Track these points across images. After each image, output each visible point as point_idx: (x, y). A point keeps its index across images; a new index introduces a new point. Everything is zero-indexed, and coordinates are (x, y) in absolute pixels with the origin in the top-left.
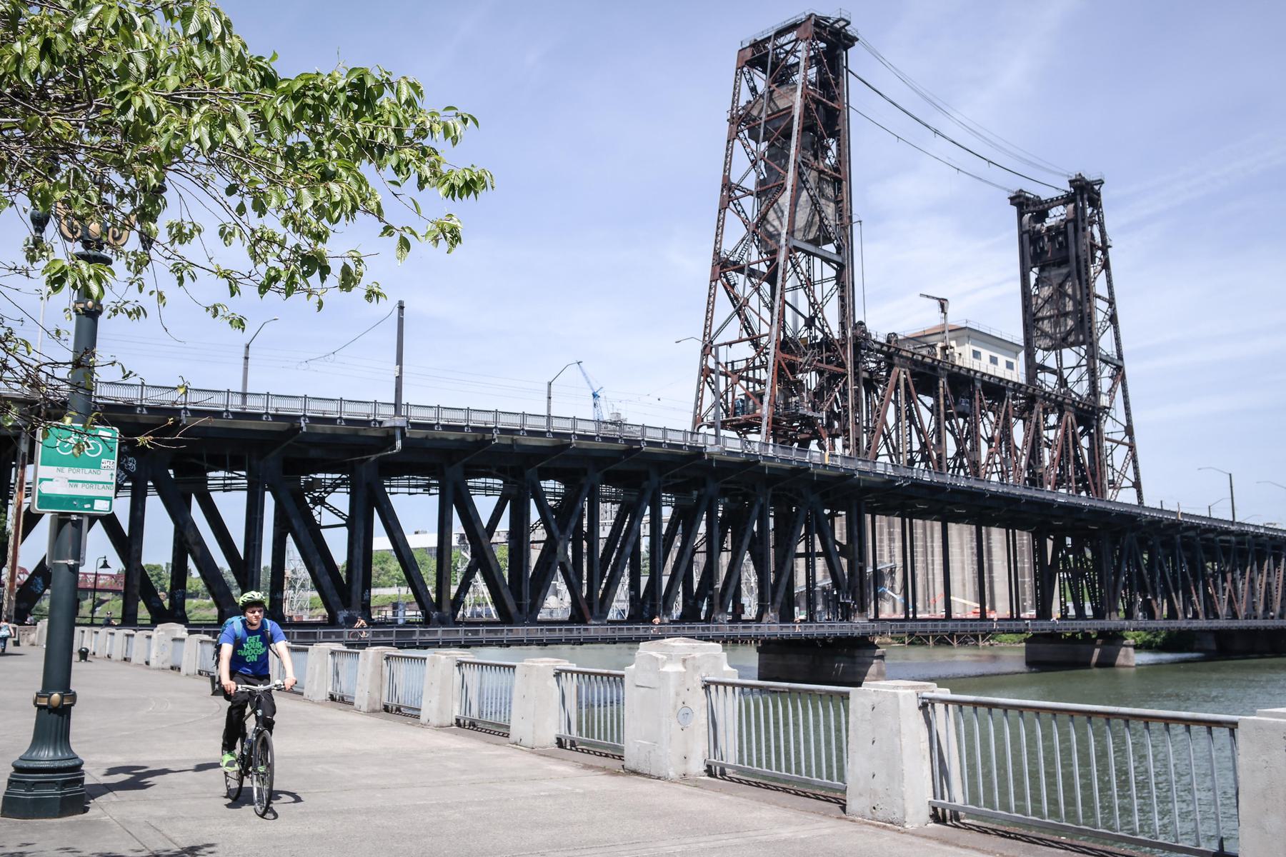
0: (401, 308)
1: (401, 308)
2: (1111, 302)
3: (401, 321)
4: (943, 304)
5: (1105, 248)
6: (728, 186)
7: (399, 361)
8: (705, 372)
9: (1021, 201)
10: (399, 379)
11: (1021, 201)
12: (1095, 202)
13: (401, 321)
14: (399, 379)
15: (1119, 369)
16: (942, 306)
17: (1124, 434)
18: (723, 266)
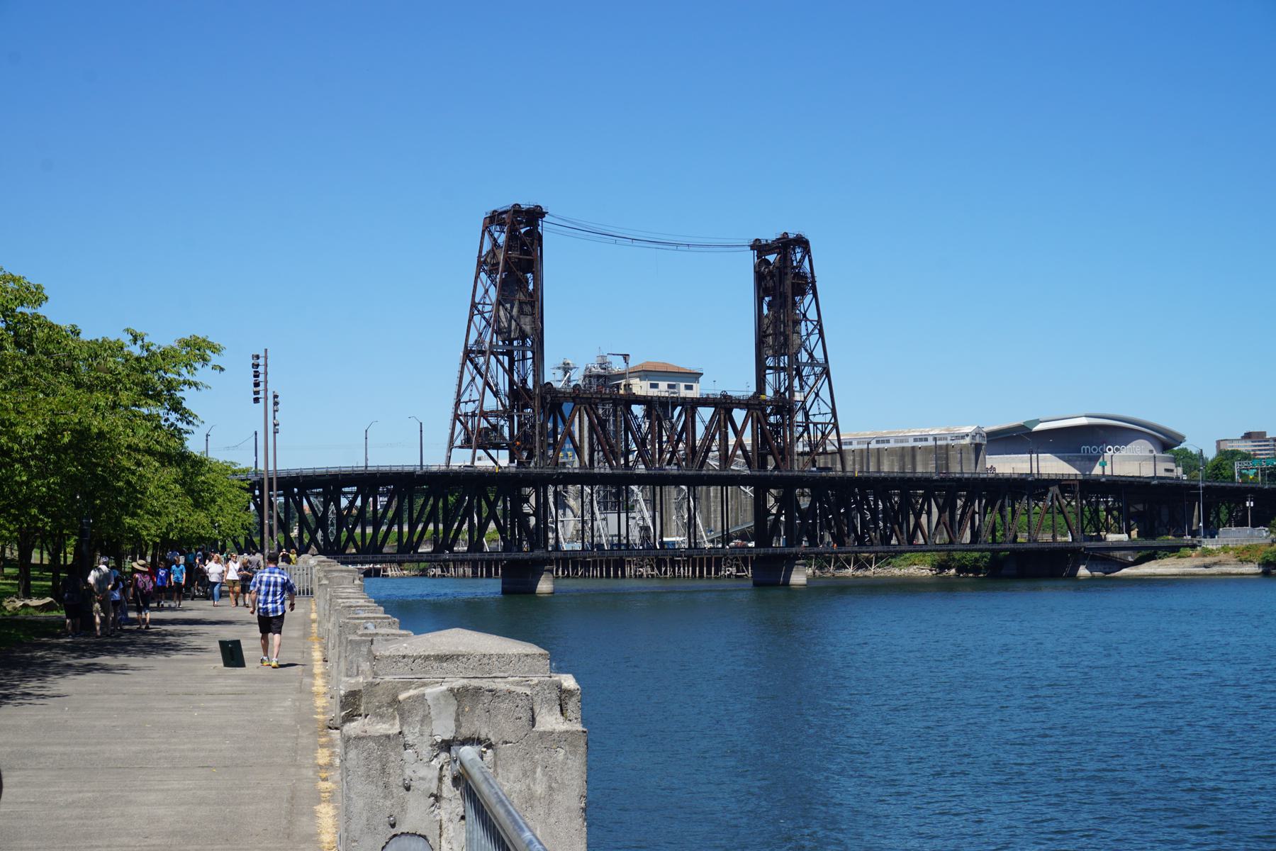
0: (256, 434)
1: (256, 434)
2: (819, 321)
3: (256, 439)
4: (626, 357)
5: (814, 283)
6: (474, 305)
7: (256, 455)
8: (456, 417)
9: (760, 248)
10: (256, 462)
11: (760, 248)
12: (807, 251)
13: (256, 439)
14: (256, 462)
15: (826, 371)
16: (625, 359)
17: (831, 415)
18: (468, 354)
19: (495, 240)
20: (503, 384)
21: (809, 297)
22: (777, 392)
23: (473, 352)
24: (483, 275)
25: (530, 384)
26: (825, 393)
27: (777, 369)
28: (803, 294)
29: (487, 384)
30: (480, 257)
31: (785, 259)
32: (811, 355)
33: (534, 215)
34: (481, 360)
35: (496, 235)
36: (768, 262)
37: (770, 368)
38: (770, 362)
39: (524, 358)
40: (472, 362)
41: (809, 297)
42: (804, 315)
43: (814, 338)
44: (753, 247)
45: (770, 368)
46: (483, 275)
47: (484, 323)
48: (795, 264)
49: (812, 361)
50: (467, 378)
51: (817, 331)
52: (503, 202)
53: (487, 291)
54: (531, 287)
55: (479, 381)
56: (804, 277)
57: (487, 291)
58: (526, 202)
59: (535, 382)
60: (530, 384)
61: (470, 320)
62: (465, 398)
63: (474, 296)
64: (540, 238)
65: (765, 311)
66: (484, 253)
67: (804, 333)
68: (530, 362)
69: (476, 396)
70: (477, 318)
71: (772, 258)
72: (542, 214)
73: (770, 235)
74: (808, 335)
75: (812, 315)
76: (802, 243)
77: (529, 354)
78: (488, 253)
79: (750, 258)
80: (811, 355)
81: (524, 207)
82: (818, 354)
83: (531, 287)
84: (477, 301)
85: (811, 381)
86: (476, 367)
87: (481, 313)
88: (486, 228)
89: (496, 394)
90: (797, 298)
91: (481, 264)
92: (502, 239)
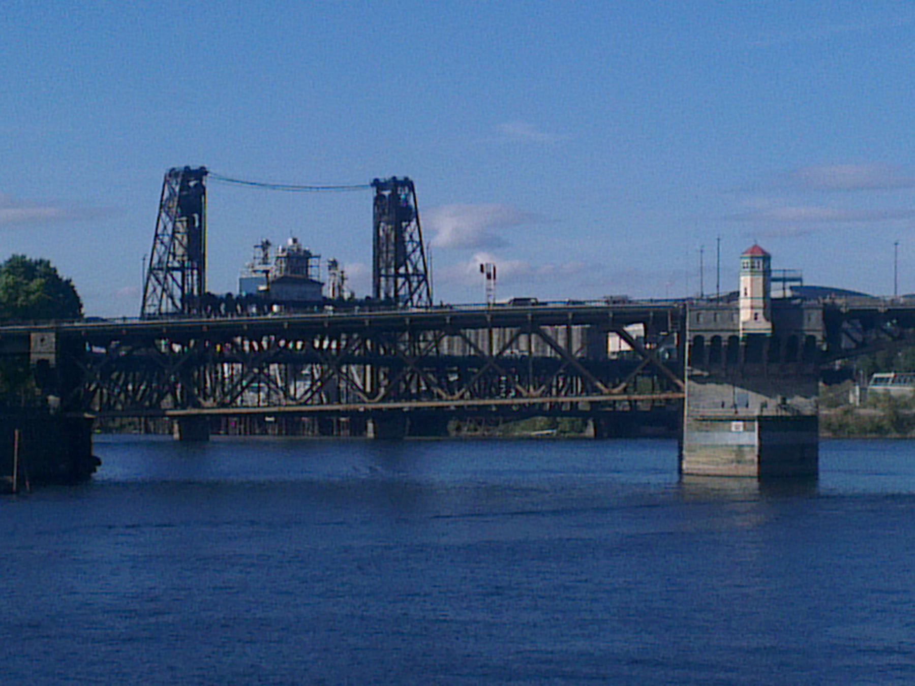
2: (421, 243)
6: (157, 235)
9: (376, 183)
12: (412, 189)
19: (173, 189)
20: (177, 293)
21: (414, 224)
22: (387, 295)
23: (155, 269)
24: (163, 215)
25: (196, 292)
26: (424, 295)
27: (387, 276)
28: (410, 221)
29: (164, 290)
30: (162, 200)
31: (395, 195)
32: (415, 268)
33: (202, 173)
34: (161, 276)
35: (174, 186)
36: (384, 196)
37: (383, 276)
38: (383, 272)
39: (192, 274)
40: (154, 275)
41: (414, 224)
42: (411, 236)
43: (418, 253)
44: (372, 185)
45: (383, 276)
46: (163, 215)
47: (163, 248)
48: (403, 197)
49: (416, 273)
50: (150, 289)
51: (419, 249)
52: (180, 165)
53: (165, 228)
54: (197, 224)
55: (159, 289)
56: (410, 208)
57: (165, 228)
58: (194, 166)
59: (199, 291)
60: (196, 292)
61: (154, 248)
62: (149, 302)
63: (157, 229)
64: (204, 188)
65: (381, 233)
66: (165, 197)
67: (410, 248)
68: (195, 277)
69: (156, 302)
70: (158, 246)
71: (387, 193)
72: (206, 173)
73: (385, 176)
74: (414, 251)
75: (416, 238)
76: (409, 184)
77: (195, 272)
78: (167, 199)
79: (372, 193)
80: (415, 268)
81: (192, 168)
82: (421, 267)
83: (197, 224)
84: (159, 232)
85: (415, 284)
86: (157, 280)
87: (162, 243)
88: (166, 181)
89: (171, 297)
90: (404, 224)
91: (161, 207)
92: (177, 189)
